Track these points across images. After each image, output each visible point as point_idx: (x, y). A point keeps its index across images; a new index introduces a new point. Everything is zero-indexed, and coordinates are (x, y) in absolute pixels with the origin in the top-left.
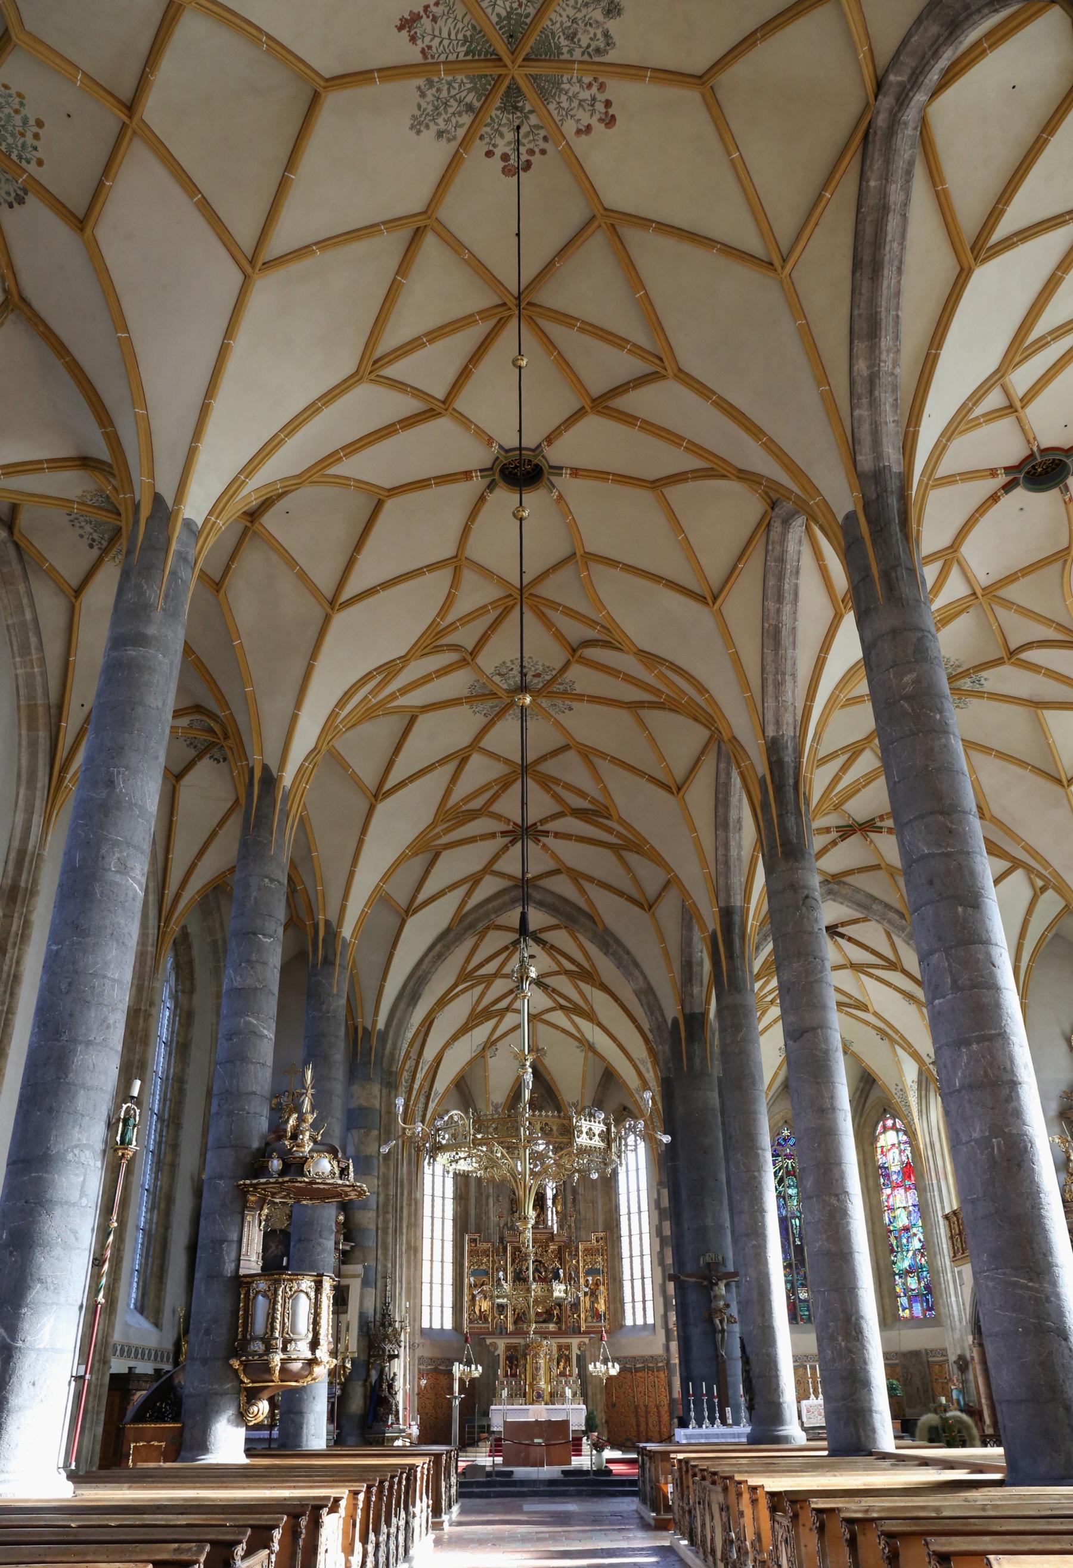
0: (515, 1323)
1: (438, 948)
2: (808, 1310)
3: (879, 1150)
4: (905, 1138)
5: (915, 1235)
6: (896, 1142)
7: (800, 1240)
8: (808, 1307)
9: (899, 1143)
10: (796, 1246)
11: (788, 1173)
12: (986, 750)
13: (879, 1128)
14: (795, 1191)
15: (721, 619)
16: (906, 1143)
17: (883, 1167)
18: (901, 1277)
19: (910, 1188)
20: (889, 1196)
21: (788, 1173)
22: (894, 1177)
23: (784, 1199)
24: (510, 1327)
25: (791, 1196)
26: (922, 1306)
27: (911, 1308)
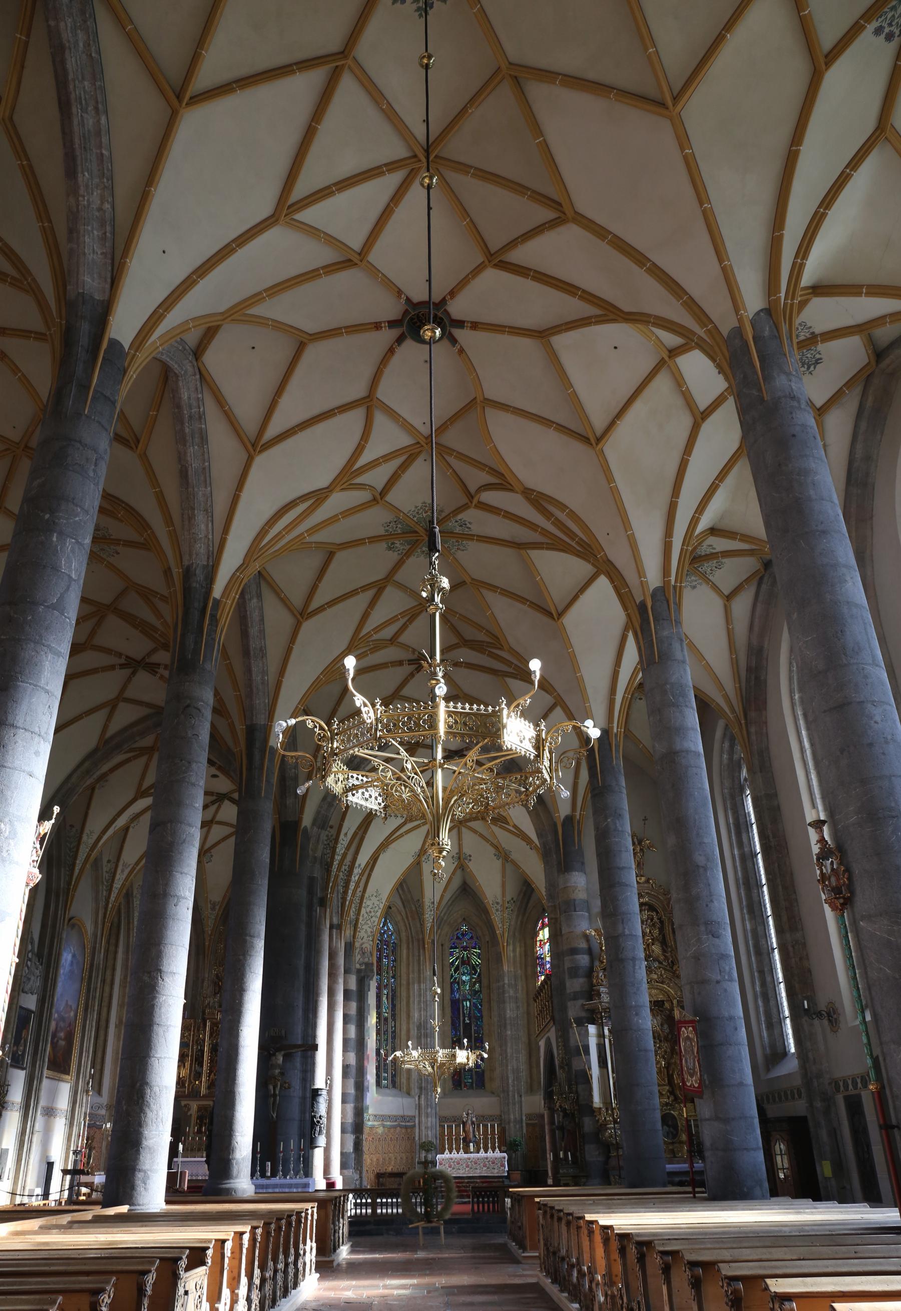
0: (209, 1088)
1: (87, 764)
2: (471, 1078)
3: (538, 944)
7: (469, 1019)
8: (472, 1076)
10: (466, 1025)
12: (493, 588)
15: (144, 458)
24: (203, 1091)
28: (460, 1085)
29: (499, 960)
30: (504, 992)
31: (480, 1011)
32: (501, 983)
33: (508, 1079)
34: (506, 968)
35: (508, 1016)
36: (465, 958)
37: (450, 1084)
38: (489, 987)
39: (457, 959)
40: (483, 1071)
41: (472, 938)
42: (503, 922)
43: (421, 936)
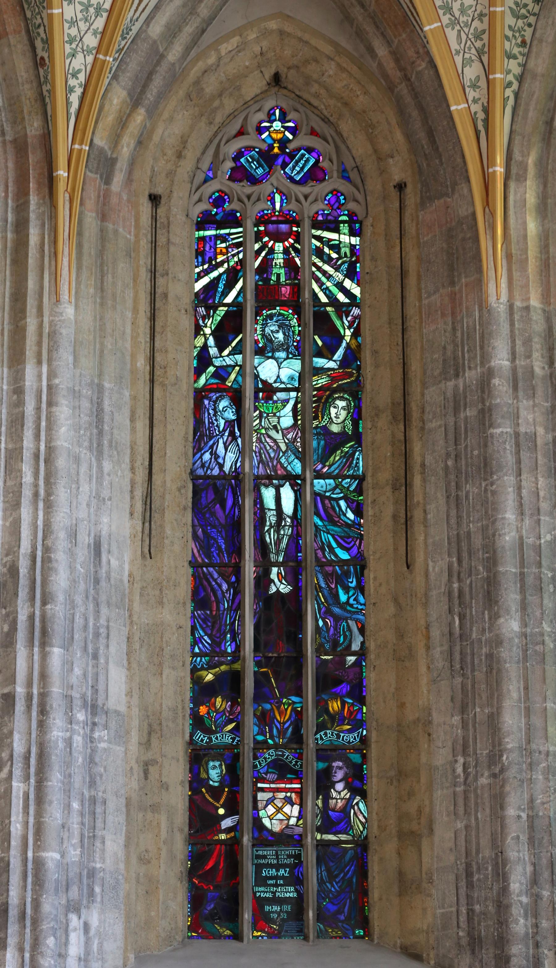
7: (294, 575)
8: (298, 863)
10: (267, 601)
11: (267, 296)
14: (291, 369)
21: (267, 296)
23: (237, 398)
25: (267, 390)
28: (230, 913)
29: (461, 255)
30: (486, 417)
31: (351, 536)
32: (471, 375)
33: (501, 874)
34: (497, 293)
35: (508, 538)
36: (279, 271)
37: (174, 904)
38: (403, 413)
39: (233, 276)
40: (362, 846)
41: (315, 174)
42: (486, 56)
43: (33, 128)
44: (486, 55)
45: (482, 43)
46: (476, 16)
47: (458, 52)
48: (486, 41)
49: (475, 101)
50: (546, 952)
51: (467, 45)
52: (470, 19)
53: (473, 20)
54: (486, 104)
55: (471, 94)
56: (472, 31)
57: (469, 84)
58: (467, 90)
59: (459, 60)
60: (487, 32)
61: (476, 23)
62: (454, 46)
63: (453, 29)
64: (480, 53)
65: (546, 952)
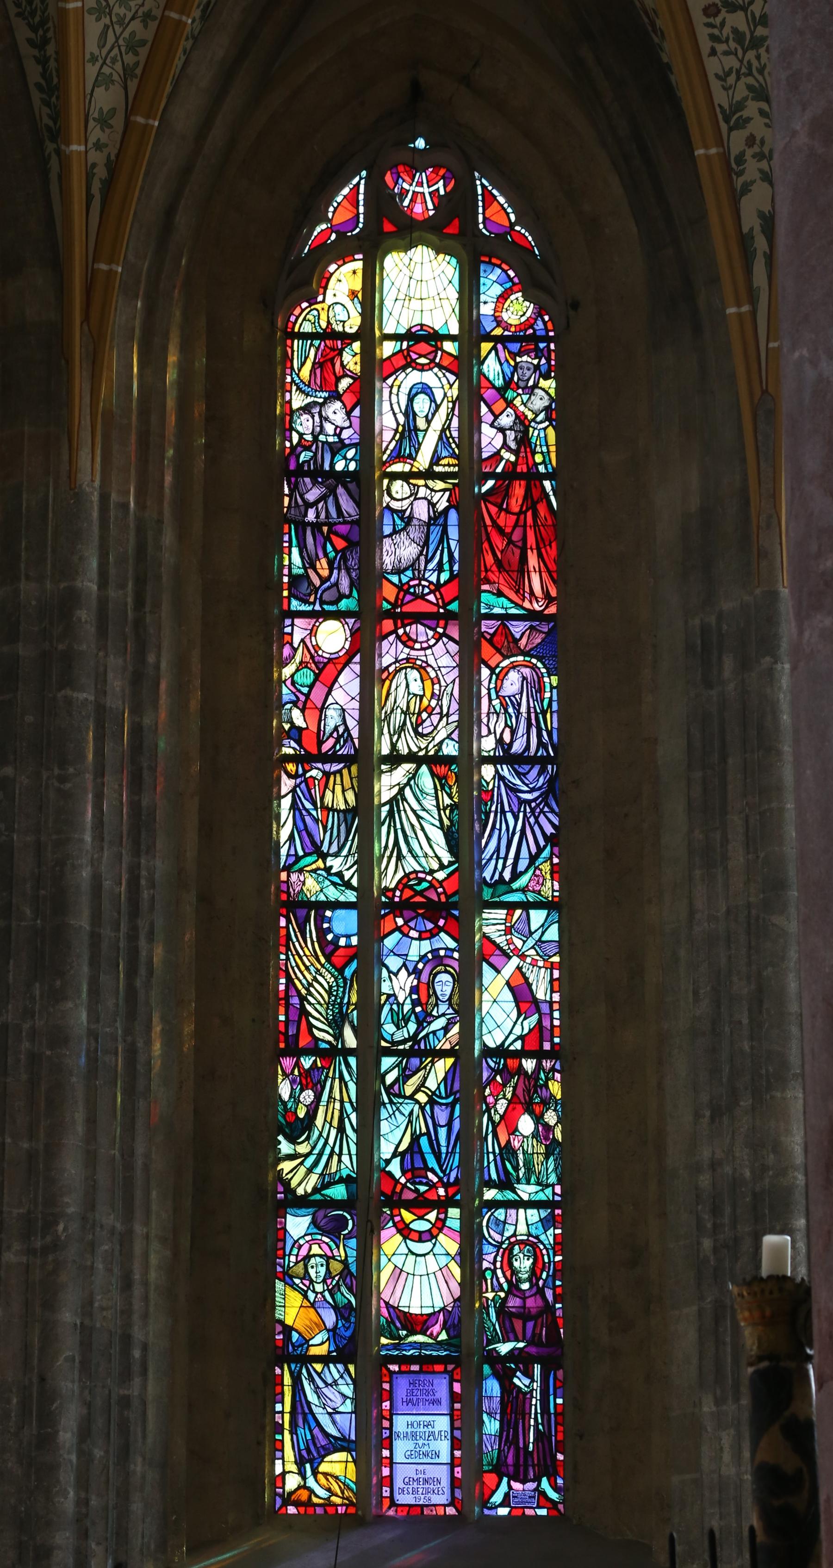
3: (304, 362)
4: (518, 311)
5: (492, 953)
6: (444, 317)
9: (472, 332)
13: (347, 203)
16: (522, 340)
17: (318, 474)
18: (329, 1226)
19: (506, 645)
20: (326, 670)
22: (397, 551)
26: (464, 1434)
27: (370, 1442)
44: (136, 81)
45: (136, 59)
46: (140, 13)
47: (94, 59)
48: (142, 58)
49: (98, 146)
50: (93, 1546)
51: (112, 54)
52: (129, 15)
53: (133, 18)
54: (113, 157)
55: (96, 133)
56: (126, 34)
57: (96, 115)
58: (92, 124)
59: (92, 71)
60: (149, 44)
61: (136, 26)
62: (92, 46)
63: (98, 19)
64: (128, 72)
65: (93, 1546)
